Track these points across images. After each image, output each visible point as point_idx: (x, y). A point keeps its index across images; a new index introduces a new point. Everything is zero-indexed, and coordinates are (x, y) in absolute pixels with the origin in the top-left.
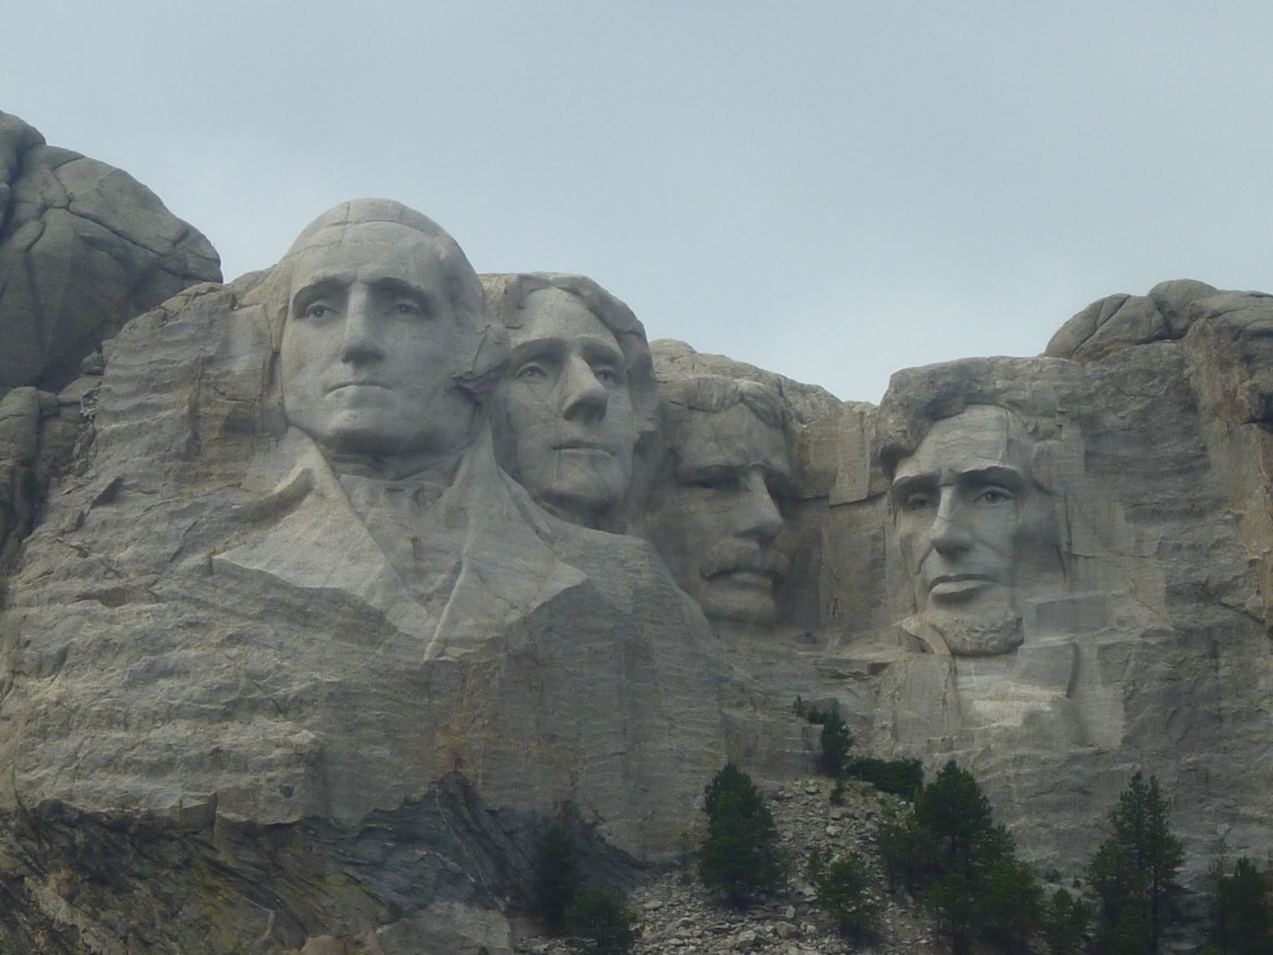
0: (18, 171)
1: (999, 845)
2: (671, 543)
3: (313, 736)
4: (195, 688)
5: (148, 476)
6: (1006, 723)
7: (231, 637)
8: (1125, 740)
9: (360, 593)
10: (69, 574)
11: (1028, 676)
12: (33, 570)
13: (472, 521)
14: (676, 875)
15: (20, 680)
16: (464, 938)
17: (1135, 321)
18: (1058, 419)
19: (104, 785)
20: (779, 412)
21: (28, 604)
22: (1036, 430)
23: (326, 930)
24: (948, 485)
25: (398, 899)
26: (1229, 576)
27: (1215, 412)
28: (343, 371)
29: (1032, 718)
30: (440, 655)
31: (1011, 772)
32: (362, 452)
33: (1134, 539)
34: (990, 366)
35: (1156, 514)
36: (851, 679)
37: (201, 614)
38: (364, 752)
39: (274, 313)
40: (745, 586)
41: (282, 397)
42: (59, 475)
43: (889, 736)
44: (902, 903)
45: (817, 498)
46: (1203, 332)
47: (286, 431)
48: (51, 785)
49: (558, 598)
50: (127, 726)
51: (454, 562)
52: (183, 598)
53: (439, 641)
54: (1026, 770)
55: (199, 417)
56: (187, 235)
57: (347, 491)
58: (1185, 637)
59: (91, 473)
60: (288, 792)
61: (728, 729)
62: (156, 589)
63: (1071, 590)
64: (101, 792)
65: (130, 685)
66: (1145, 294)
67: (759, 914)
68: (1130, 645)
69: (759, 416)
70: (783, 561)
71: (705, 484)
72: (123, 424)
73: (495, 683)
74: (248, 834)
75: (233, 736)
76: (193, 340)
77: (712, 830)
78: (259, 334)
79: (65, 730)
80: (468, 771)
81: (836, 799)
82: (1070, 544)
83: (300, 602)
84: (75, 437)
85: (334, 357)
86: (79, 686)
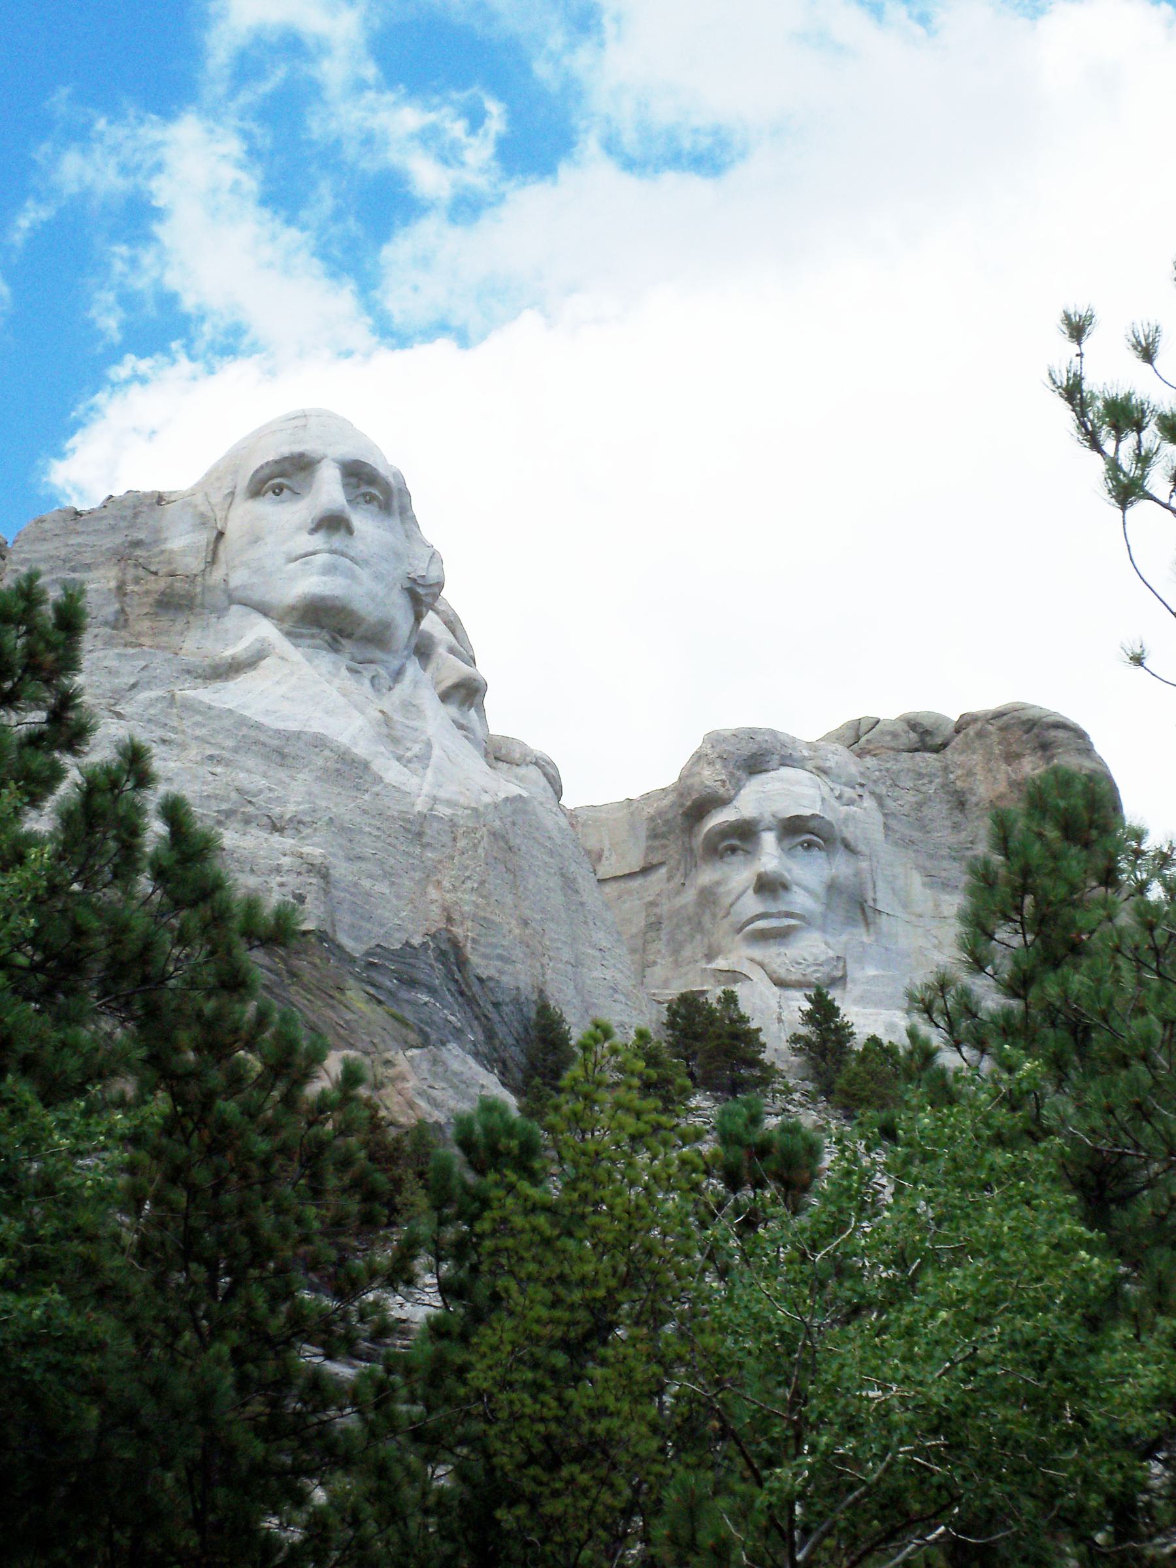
7: (211, 757)
9: (344, 739)
16: (483, 1086)
18: (860, 790)
22: (839, 797)
24: (769, 829)
32: (326, 624)
33: (931, 904)
38: (366, 883)
47: (227, 609)
52: (149, 721)
55: (125, 594)
62: (118, 708)
73: (480, 850)
78: (202, 515)
80: (458, 931)
82: (875, 900)
83: (276, 743)
85: (299, 528)
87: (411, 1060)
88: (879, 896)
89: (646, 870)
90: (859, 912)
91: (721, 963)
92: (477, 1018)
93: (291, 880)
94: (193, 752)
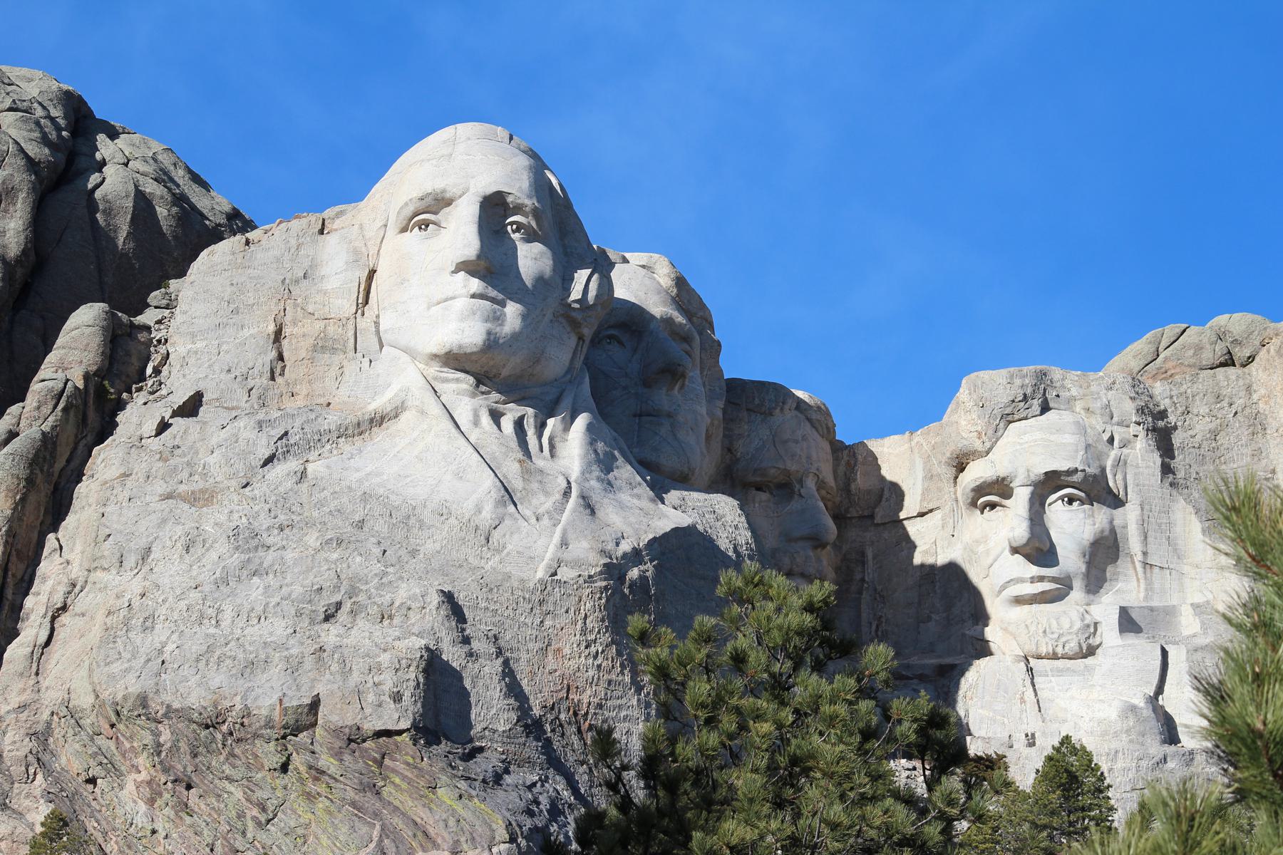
3: (423, 642)
17: (1199, 348)
18: (1134, 429)
20: (830, 425)
22: (1111, 440)
30: (555, 574)
36: (915, 681)
41: (378, 317)
45: (862, 517)
51: (564, 484)
53: (552, 560)
54: (1120, 764)
60: (397, 698)
69: (813, 426)
71: (759, 489)
74: (354, 739)
78: (356, 252)
88: (1152, 548)
90: (1130, 565)
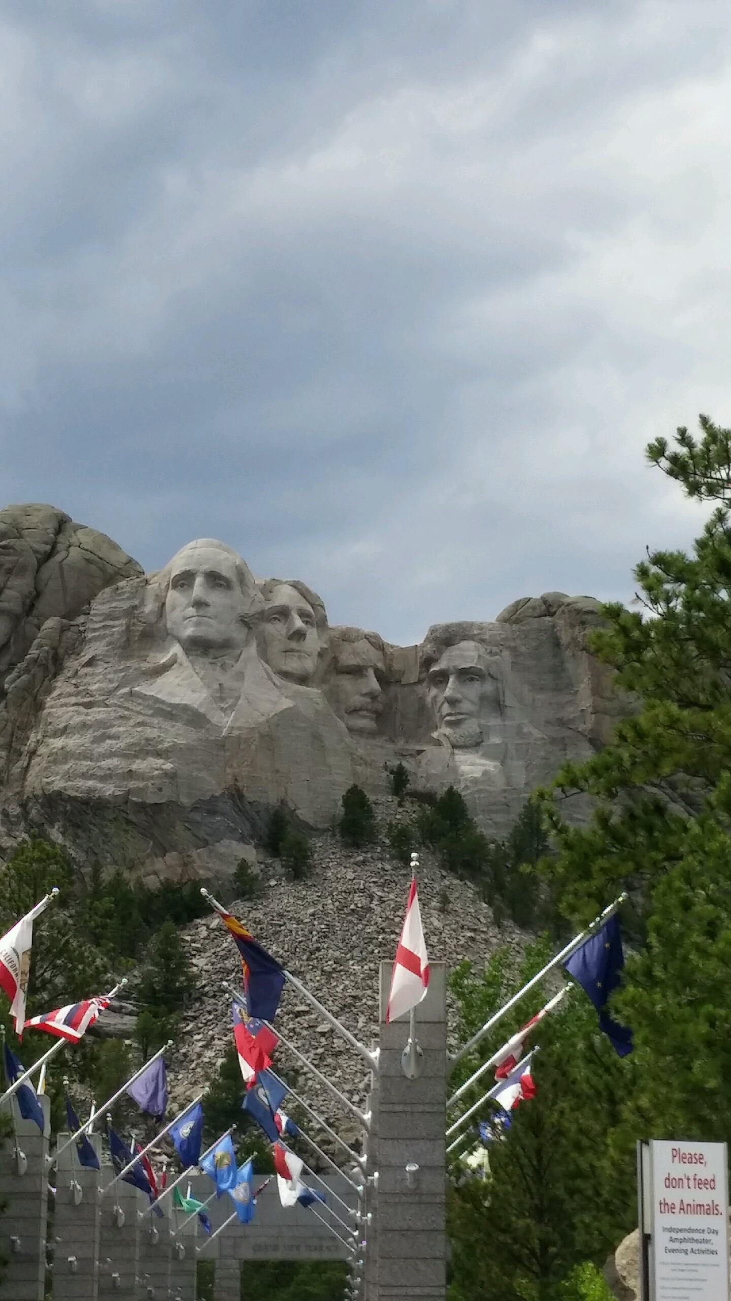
0: (59, 530)
1: (471, 826)
2: (333, 697)
4: (121, 744)
5: (104, 655)
6: (475, 775)
8: (527, 784)
9: (196, 706)
10: (70, 695)
11: (486, 756)
12: (55, 693)
13: (246, 678)
14: (330, 833)
15: (46, 739)
17: (534, 608)
19: (80, 784)
21: (52, 707)
23: (174, 848)
25: (206, 837)
26: (572, 716)
27: (568, 647)
28: (191, 611)
29: (485, 773)
31: (477, 796)
32: (200, 647)
34: (472, 625)
35: (542, 689)
37: (126, 713)
38: (194, 774)
39: (163, 586)
40: (364, 717)
42: (69, 655)
43: (424, 780)
44: (428, 848)
46: (563, 612)
48: (58, 784)
49: (281, 712)
50: (91, 760)
51: (237, 695)
52: (120, 706)
56: (130, 561)
57: (192, 662)
58: (553, 741)
59: (83, 654)
61: (355, 774)
62: (107, 702)
63: (504, 720)
64: (80, 787)
65: (93, 742)
66: (538, 597)
67: (365, 850)
68: (529, 744)
70: (380, 707)
71: (348, 673)
72: (97, 634)
73: (253, 747)
74: (142, 807)
75: (139, 765)
76: (128, 598)
77: (346, 814)
79: (65, 760)
81: (400, 805)
83: (169, 709)
84: (77, 639)
85: (188, 606)
86: (71, 742)
87: (199, 854)
88: (507, 699)
89: (420, 681)
91: (435, 735)
92: (248, 820)
93: (157, 782)
94: (132, 722)
